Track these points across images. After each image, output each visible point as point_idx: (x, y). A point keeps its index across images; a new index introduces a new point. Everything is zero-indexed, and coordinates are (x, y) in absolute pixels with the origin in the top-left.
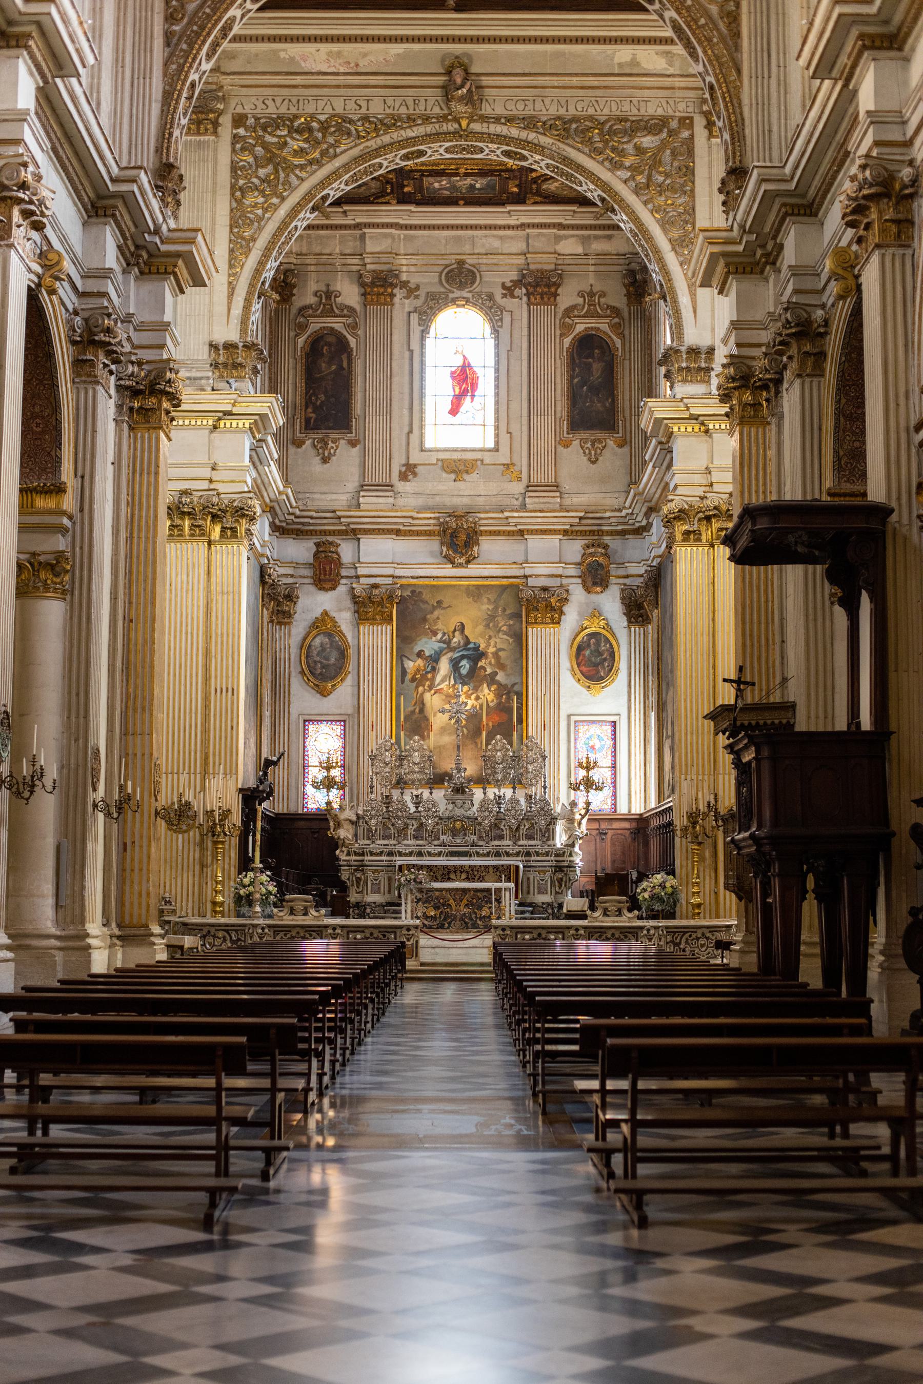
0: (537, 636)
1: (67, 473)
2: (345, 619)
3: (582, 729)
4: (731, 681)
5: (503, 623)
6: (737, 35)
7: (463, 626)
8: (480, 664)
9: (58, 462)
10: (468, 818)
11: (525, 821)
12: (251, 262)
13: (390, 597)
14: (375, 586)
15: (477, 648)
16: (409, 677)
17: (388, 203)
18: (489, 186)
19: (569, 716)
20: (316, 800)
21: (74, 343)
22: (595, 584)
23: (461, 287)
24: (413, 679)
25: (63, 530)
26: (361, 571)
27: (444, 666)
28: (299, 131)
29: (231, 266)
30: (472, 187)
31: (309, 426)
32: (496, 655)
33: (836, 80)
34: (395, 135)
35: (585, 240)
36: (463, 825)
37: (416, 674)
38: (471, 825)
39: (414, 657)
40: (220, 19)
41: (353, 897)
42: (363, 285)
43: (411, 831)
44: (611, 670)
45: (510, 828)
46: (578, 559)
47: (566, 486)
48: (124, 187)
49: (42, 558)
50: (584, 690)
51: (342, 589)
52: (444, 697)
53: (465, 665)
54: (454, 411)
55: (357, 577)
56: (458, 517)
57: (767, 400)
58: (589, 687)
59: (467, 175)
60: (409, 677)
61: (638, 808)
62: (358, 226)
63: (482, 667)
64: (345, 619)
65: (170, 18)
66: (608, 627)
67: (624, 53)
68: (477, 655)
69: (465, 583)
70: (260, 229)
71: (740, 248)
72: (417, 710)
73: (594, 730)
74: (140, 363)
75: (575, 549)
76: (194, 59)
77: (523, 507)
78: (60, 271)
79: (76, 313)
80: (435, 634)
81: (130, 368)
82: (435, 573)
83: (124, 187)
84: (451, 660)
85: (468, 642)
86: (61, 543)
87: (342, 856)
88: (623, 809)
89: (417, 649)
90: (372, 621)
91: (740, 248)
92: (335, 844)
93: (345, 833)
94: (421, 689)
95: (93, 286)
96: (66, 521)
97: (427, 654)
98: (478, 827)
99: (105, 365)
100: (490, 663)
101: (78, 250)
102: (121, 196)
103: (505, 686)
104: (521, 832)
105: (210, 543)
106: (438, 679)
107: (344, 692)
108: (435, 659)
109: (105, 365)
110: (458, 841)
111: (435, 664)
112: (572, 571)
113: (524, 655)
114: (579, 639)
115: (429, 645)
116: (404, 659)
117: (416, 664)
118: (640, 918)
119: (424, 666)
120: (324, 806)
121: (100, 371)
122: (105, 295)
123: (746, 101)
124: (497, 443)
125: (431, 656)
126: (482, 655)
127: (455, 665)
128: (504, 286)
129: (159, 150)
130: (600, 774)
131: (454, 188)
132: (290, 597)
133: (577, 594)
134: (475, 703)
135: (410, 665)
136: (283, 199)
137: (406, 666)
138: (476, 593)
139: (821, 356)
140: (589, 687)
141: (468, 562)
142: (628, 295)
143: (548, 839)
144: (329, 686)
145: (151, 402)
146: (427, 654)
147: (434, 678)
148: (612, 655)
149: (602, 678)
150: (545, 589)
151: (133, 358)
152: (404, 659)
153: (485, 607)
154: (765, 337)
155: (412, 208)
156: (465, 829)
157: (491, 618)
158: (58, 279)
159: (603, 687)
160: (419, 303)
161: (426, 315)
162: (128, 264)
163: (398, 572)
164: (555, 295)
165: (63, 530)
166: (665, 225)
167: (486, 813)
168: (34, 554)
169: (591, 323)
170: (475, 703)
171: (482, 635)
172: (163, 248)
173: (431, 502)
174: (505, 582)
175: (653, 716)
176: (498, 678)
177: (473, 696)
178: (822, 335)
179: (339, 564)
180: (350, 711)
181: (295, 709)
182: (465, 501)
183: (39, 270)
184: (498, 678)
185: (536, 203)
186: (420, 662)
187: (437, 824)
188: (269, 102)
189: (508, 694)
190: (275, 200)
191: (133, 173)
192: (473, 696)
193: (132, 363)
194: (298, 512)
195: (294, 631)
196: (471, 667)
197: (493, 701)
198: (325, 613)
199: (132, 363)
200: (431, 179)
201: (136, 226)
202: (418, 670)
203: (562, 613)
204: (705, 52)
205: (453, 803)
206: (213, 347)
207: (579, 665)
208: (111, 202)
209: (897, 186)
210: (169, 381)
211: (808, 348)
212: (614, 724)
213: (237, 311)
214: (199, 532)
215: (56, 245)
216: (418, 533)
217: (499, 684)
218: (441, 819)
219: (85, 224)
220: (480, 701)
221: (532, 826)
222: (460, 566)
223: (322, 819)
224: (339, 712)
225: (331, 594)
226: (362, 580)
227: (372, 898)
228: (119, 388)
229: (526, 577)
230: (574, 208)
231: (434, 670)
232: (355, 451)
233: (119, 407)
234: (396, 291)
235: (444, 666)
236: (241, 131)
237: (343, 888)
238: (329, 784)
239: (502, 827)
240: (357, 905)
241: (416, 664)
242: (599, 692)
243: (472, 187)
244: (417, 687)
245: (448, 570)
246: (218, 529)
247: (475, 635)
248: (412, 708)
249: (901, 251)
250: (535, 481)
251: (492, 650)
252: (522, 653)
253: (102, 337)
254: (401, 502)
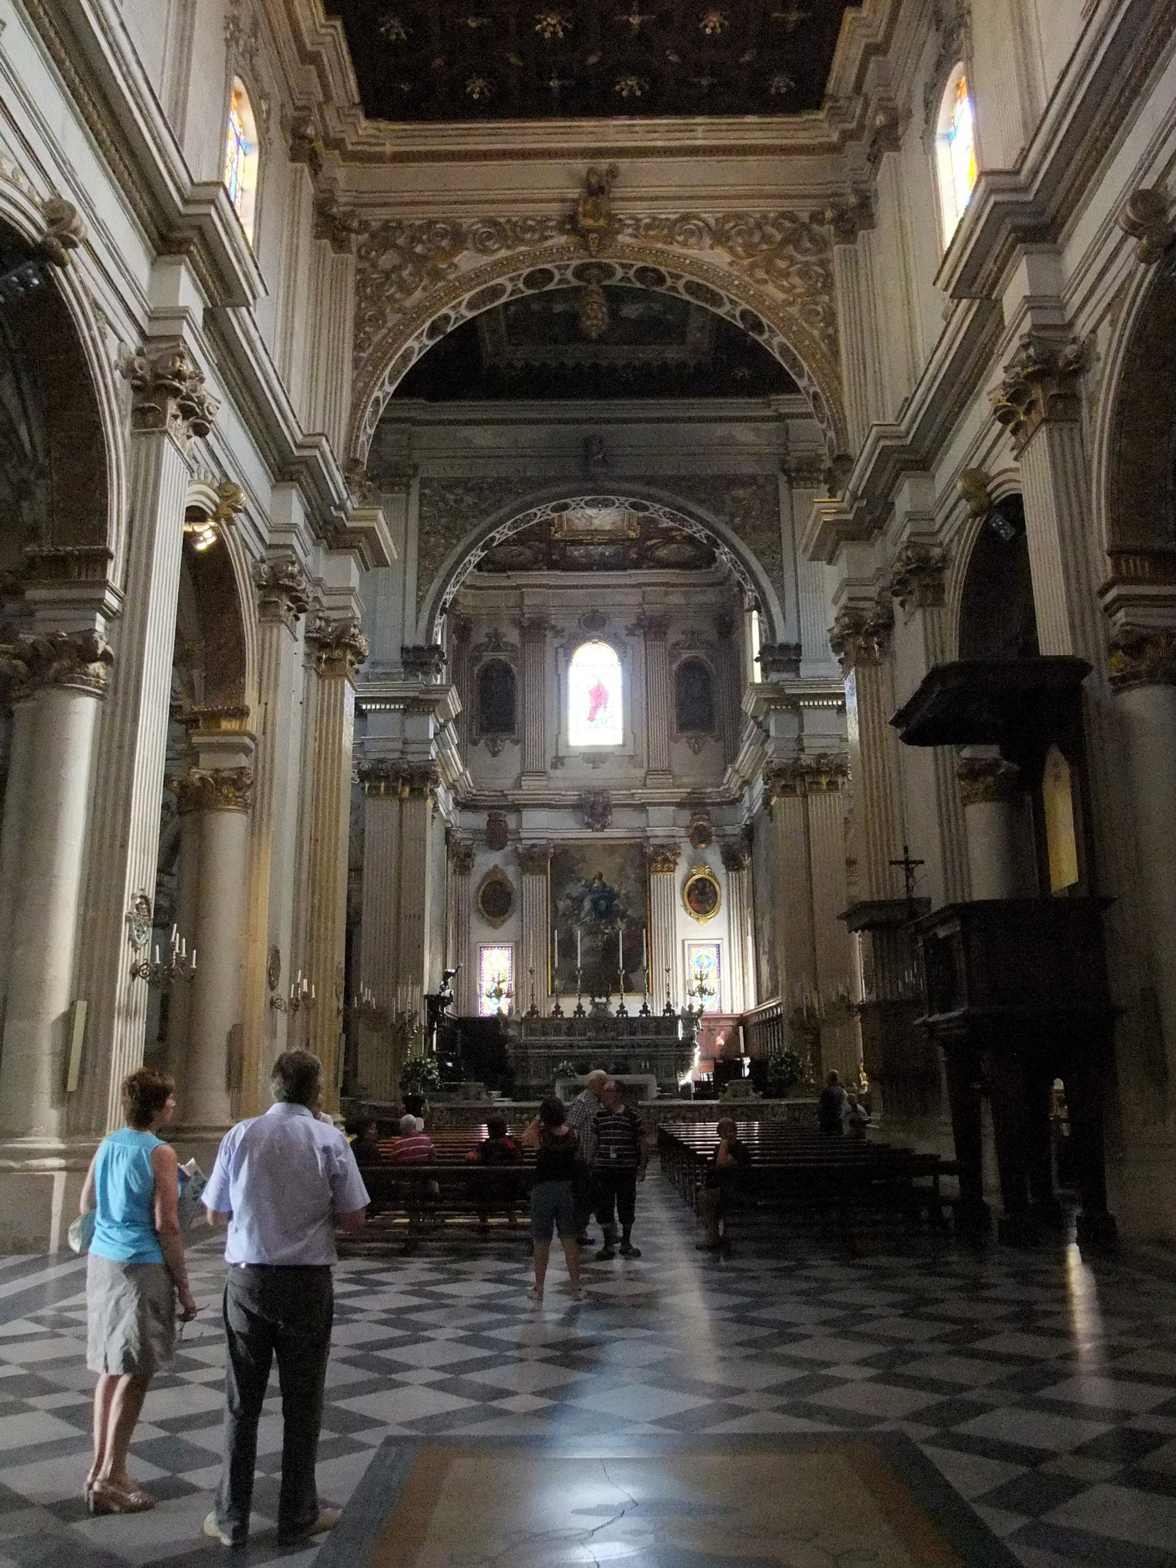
0: (657, 881)
1: (250, 698)
2: (511, 872)
3: (693, 950)
4: (901, 863)
5: (631, 873)
6: (836, 354)
7: (600, 876)
9: (242, 688)
12: (435, 585)
13: (545, 855)
14: (534, 846)
15: (612, 890)
17: (539, 569)
18: (615, 554)
19: (683, 941)
20: (488, 1007)
21: (260, 587)
22: (702, 842)
23: (596, 628)
24: (564, 914)
25: (246, 750)
26: (523, 835)
27: (587, 905)
28: (472, 490)
29: (418, 589)
30: (602, 555)
31: (483, 730)
32: (626, 895)
33: (974, 298)
34: (545, 492)
35: (686, 594)
40: (398, 348)
41: (519, 1082)
42: (522, 628)
43: (564, 1029)
46: (687, 823)
47: (676, 769)
48: (306, 453)
49: (225, 774)
50: (694, 921)
51: (509, 848)
53: (603, 904)
54: (591, 719)
55: (521, 839)
56: (596, 794)
57: (879, 644)
59: (600, 544)
61: (739, 1010)
62: (518, 587)
64: (511, 872)
65: (358, 347)
66: (712, 874)
67: (721, 430)
68: (611, 896)
69: (604, 842)
70: (442, 562)
71: (850, 517)
73: (703, 951)
74: (328, 621)
75: (685, 816)
76: (378, 378)
77: (645, 786)
78: (237, 502)
79: (263, 561)
80: (579, 880)
81: (318, 622)
82: (580, 836)
83: (306, 453)
84: (592, 901)
85: (604, 885)
86: (243, 760)
87: (510, 1050)
88: (727, 1011)
89: (568, 891)
90: (533, 872)
91: (850, 517)
92: (505, 1039)
93: (511, 1032)
95: (280, 539)
96: (247, 740)
99: (290, 609)
101: (267, 507)
102: (304, 461)
105: (401, 801)
107: (511, 925)
108: (579, 901)
109: (290, 609)
112: (682, 832)
114: (690, 883)
115: (575, 889)
118: (764, 1097)
120: (495, 1012)
121: (283, 611)
122: (291, 547)
123: (846, 404)
124: (624, 740)
126: (617, 896)
127: (595, 903)
128: (627, 628)
129: (347, 449)
130: (709, 984)
131: (588, 555)
132: (469, 855)
133: (686, 848)
135: (561, 905)
136: (459, 540)
138: (612, 848)
139: (940, 588)
141: (604, 827)
142: (720, 633)
145: (337, 653)
147: (579, 914)
148: (715, 894)
150: (662, 846)
151: (321, 614)
153: (618, 860)
154: (872, 592)
155: (558, 573)
157: (622, 868)
158: (237, 510)
160: (563, 641)
161: (568, 650)
162: (318, 537)
163: (550, 836)
164: (665, 634)
165: (246, 750)
166: (759, 554)
168: (217, 771)
169: (693, 653)
171: (615, 881)
172: (349, 524)
173: (575, 783)
174: (632, 841)
175: (750, 940)
176: (629, 912)
178: (940, 570)
179: (506, 830)
181: (474, 938)
182: (601, 782)
183: (217, 500)
184: (629, 912)
185: (650, 568)
186: (569, 902)
188: (448, 469)
190: (454, 541)
191: (316, 439)
193: (320, 618)
194: (474, 791)
195: (472, 881)
198: (496, 867)
199: (320, 618)
200: (572, 548)
201: (322, 499)
203: (676, 864)
204: (810, 367)
206: (404, 650)
207: (690, 902)
208: (294, 468)
209: (1061, 363)
210: (353, 635)
211: (928, 581)
212: (718, 946)
213: (423, 623)
214: (392, 791)
215: (234, 478)
216: (565, 807)
219: (273, 487)
222: (597, 830)
223: (495, 1022)
225: (501, 853)
226: (524, 842)
227: (534, 1082)
228: (308, 639)
229: (648, 838)
230: (677, 571)
232: (517, 748)
233: (308, 655)
234: (547, 632)
235: (587, 905)
236: (427, 491)
237: (511, 1074)
238: (498, 993)
240: (522, 1088)
243: (602, 555)
245: (589, 834)
246: (407, 789)
247: (609, 880)
249: (1066, 426)
250: (653, 766)
251: (623, 892)
253: (286, 582)
254: (552, 784)
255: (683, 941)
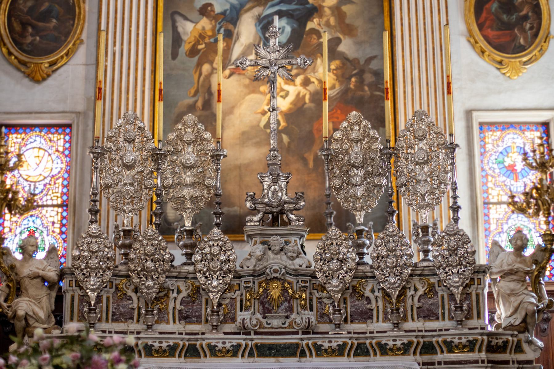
8: (310, 25)
10: (297, 273)
11: (416, 281)
16: (185, 47)
19: (469, 114)
24: (193, 52)
36: (284, 290)
37: (197, 43)
38: (303, 289)
39: (195, 15)
44: (536, 35)
45: (387, 295)
50: (492, 69)
52: (247, 81)
58: (500, 63)
60: (185, 47)
63: (314, 31)
72: (199, 104)
94: (206, 68)
97: (218, 9)
98: (316, 294)
100: (328, 24)
103: (354, 62)
104: (409, 302)
106: (237, 51)
110: (276, 323)
111: (231, 27)
113: (386, 9)
116: (179, 19)
117: (199, 26)
119: (213, 29)
125: (224, 13)
134: (303, 91)
137: (180, 30)
140: (500, 63)
143: (469, 317)
144: (45, 62)
146: (218, 9)
149: (521, 49)
152: (179, 19)
156: (289, 299)
159: (525, 63)
167: (334, 264)
170: (303, 91)
176: (342, 48)
177: (299, 80)
180: (80, 107)
184: (342, 48)
186: (205, 23)
187: (230, 288)
189: (361, 74)
192: (299, 80)
196: (293, 31)
197: (333, 87)
202: (202, 37)
205: (263, 243)
207: (481, 27)
217: (344, 58)
218: (238, 277)
220: (311, 88)
221: (431, 290)
224: (60, 108)
231: (229, 35)
239: (368, 293)
241: (199, 26)
242: (517, 71)
244: (199, 65)
248: (191, 101)
252: (382, 7)
255: (469, 114)
